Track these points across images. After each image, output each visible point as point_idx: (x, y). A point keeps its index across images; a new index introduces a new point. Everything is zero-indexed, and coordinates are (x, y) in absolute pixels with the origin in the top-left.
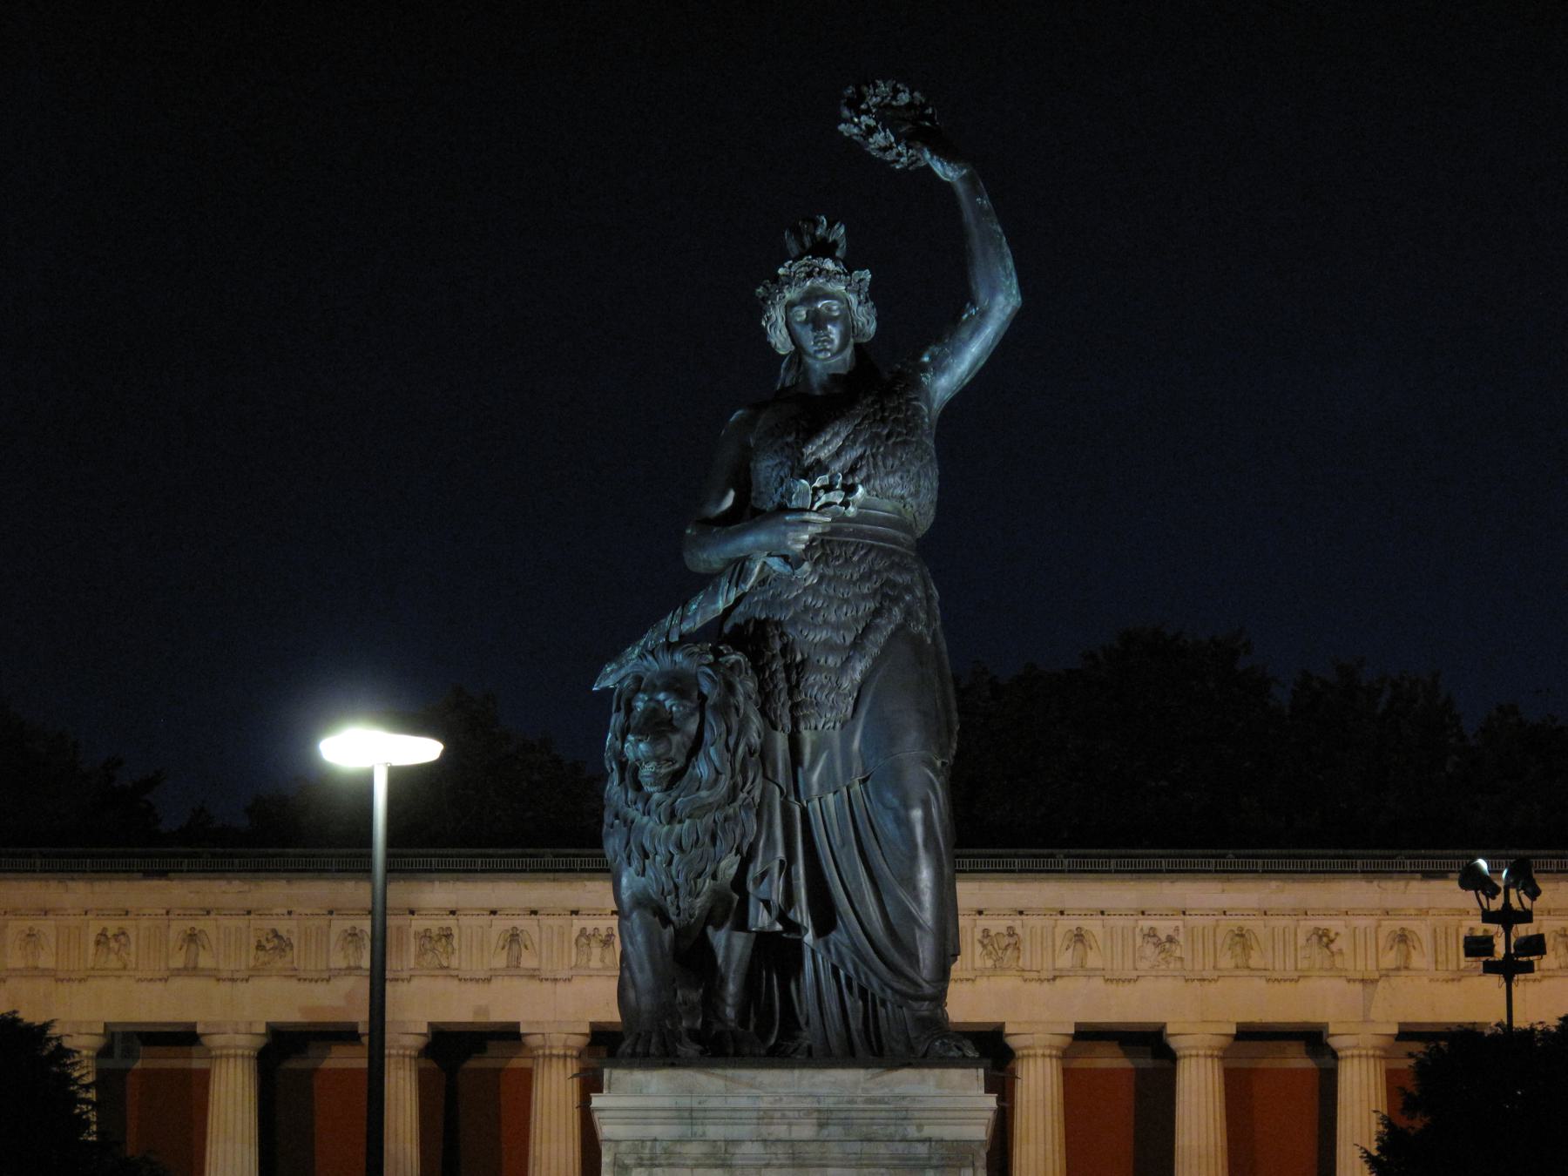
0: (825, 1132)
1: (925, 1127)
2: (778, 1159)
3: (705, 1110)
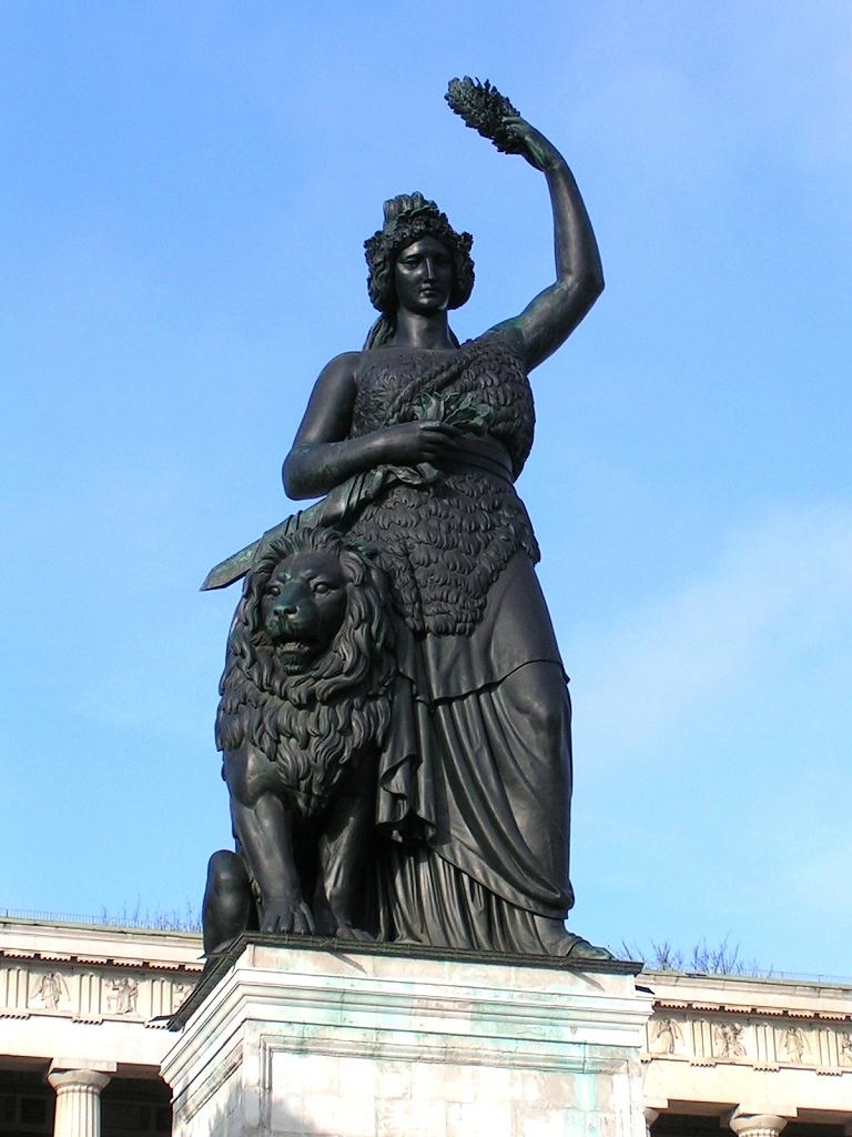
0: (479, 1029)
1: (579, 1029)
2: (430, 1053)
3: (358, 993)
